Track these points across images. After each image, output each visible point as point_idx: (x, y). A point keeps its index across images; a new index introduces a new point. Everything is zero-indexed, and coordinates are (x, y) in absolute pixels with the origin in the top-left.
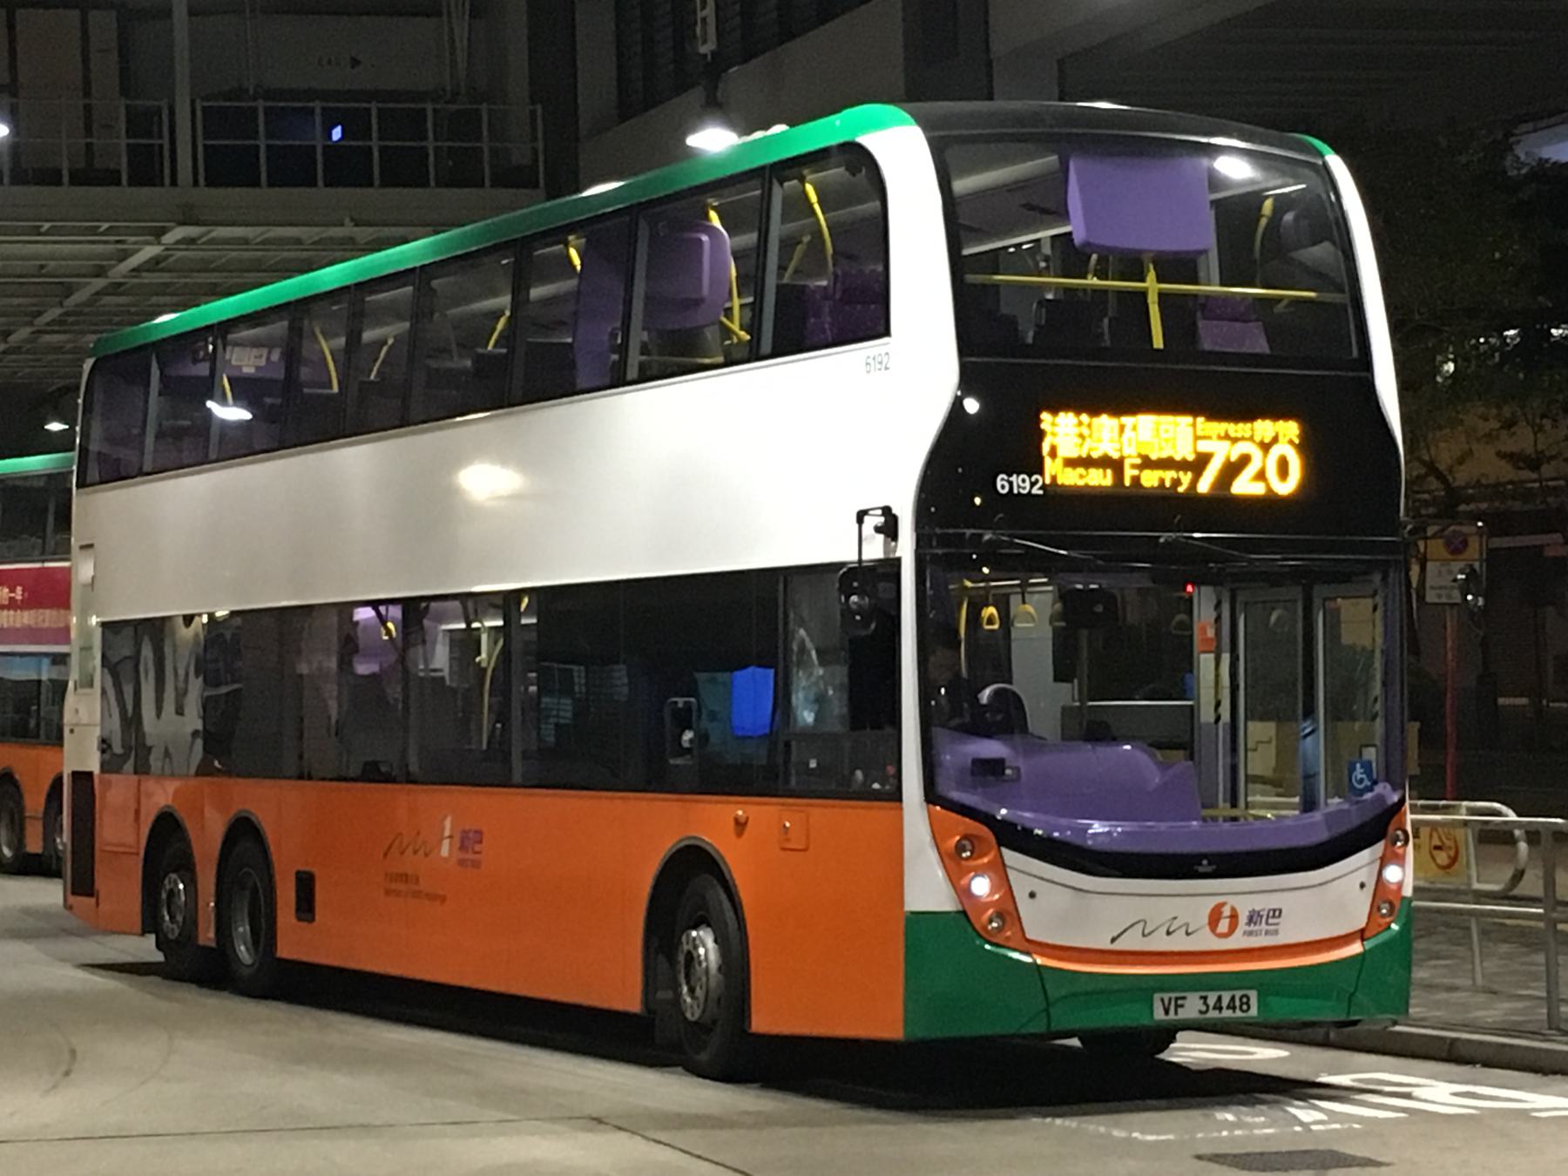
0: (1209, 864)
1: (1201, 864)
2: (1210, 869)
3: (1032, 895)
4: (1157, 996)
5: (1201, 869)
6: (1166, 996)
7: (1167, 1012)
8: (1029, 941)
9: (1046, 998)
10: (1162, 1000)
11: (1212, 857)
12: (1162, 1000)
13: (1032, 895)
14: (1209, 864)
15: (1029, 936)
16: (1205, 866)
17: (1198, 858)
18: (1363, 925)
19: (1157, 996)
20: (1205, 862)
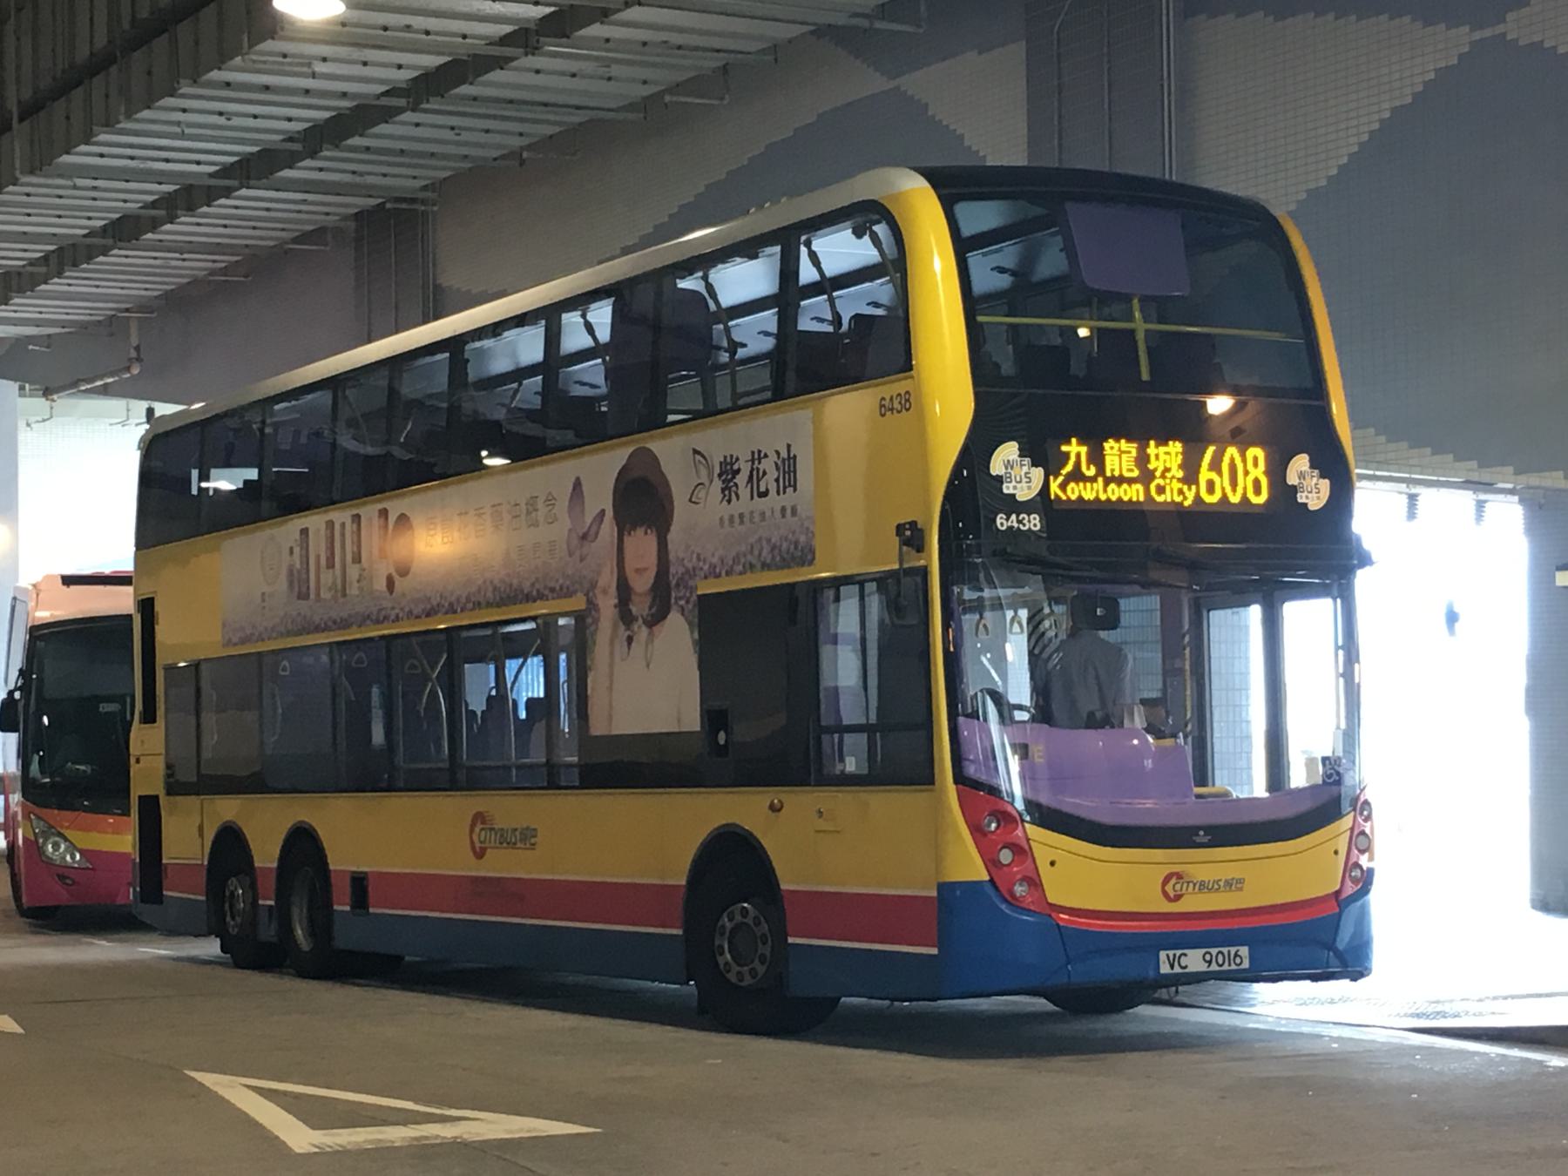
0: (1205, 835)
1: (1198, 835)
2: (1205, 840)
3: (1052, 864)
4: (1163, 954)
5: (1198, 840)
6: (1171, 953)
7: (1172, 967)
8: (1051, 905)
9: (1067, 956)
10: (1168, 956)
11: (1209, 829)
12: (1168, 956)
13: (1052, 864)
14: (1205, 835)
15: (1050, 901)
16: (1202, 837)
17: (1194, 830)
18: (1337, 887)
19: (1163, 954)
20: (1202, 833)
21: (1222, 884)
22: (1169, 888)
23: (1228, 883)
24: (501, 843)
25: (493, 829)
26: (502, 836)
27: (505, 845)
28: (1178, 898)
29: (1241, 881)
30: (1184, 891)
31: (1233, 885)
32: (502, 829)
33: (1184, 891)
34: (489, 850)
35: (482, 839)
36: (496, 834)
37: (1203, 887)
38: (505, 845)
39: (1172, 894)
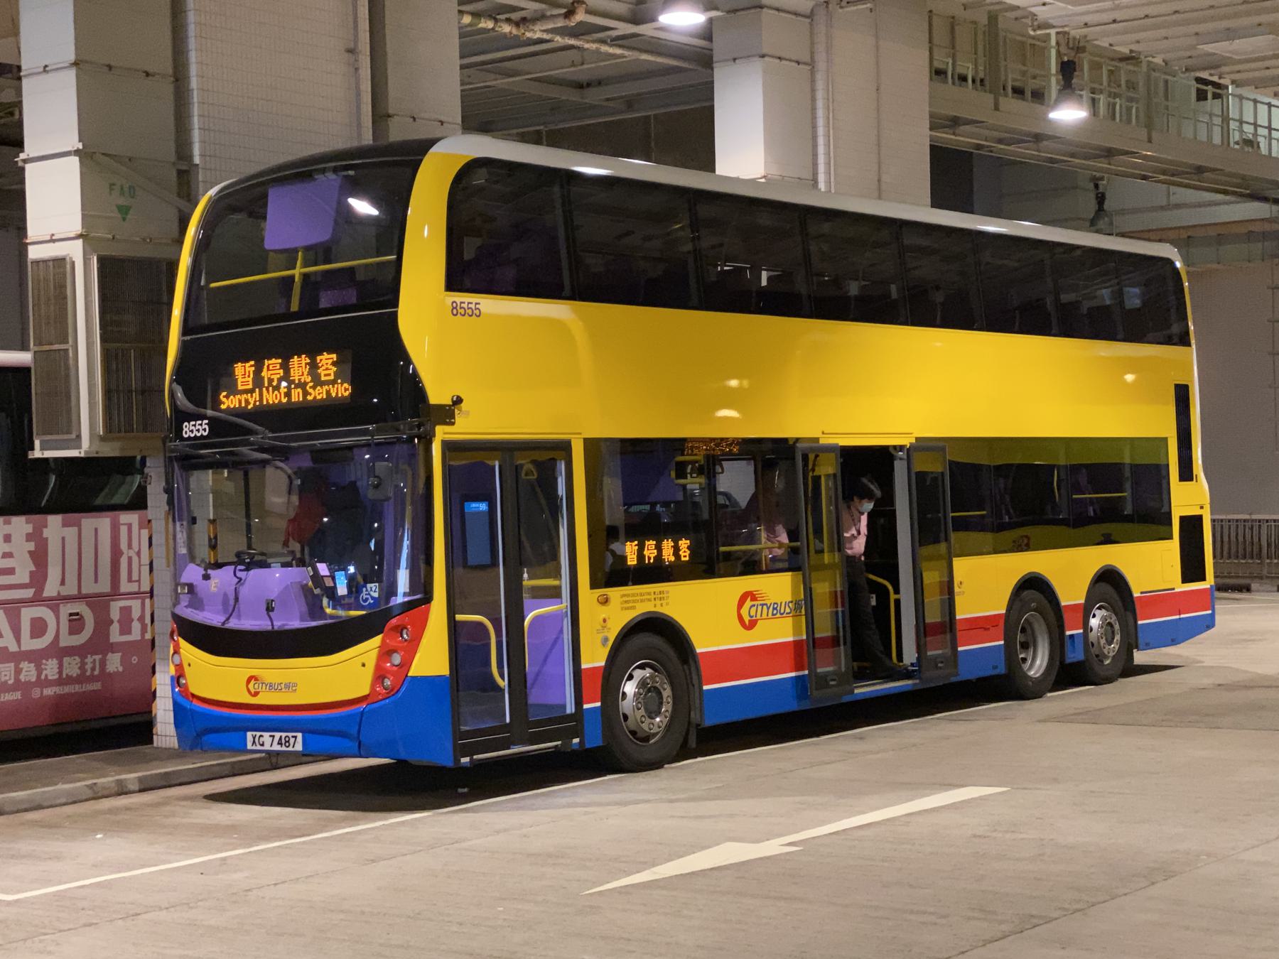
6: (254, 733)
19: (249, 734)
21: (283, 686)
22: (251, 686)
23: (287, 686)
24: (773, 615)
25: (766, 604)
26: (774, 609)
27: (778, 615)
28: (256, 694)
29: (295, 685)
30: (260, 689)
31: (289, 687)
32: (775, 604)
33: (260, 689)
34: (759, 622)
35: (753, 613)
36: (768, 609)
37: (271, 686)
38: (778, 615)
39: (253, 691)
